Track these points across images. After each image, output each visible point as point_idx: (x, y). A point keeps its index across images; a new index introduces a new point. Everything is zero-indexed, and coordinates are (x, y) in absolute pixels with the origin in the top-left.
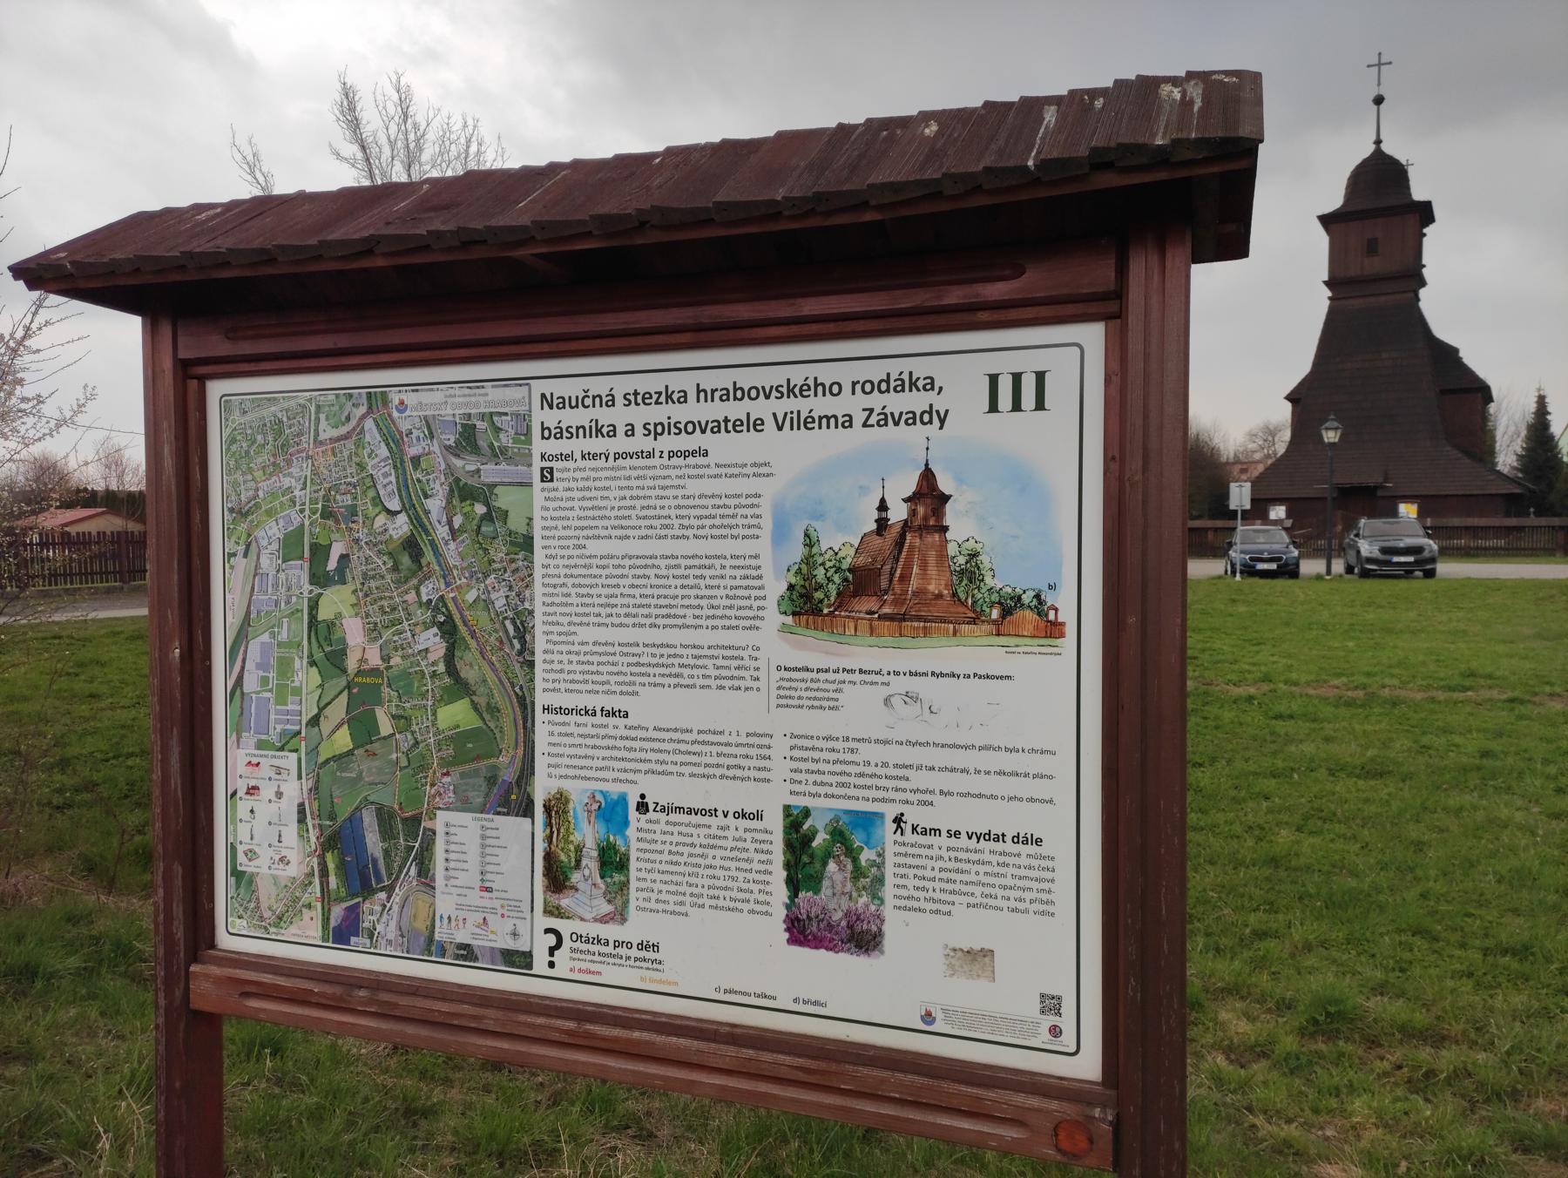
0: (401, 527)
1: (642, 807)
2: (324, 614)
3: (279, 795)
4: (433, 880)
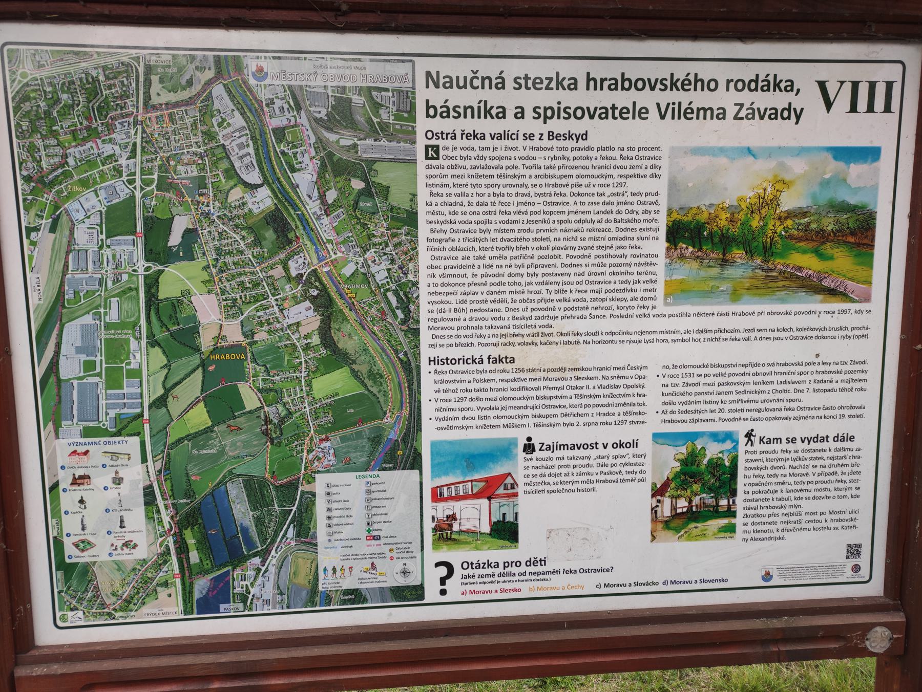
0: (262, 201)
1: (529, 448)
2: (167, 290)
3: (118, 481)
4: (314, 537)
